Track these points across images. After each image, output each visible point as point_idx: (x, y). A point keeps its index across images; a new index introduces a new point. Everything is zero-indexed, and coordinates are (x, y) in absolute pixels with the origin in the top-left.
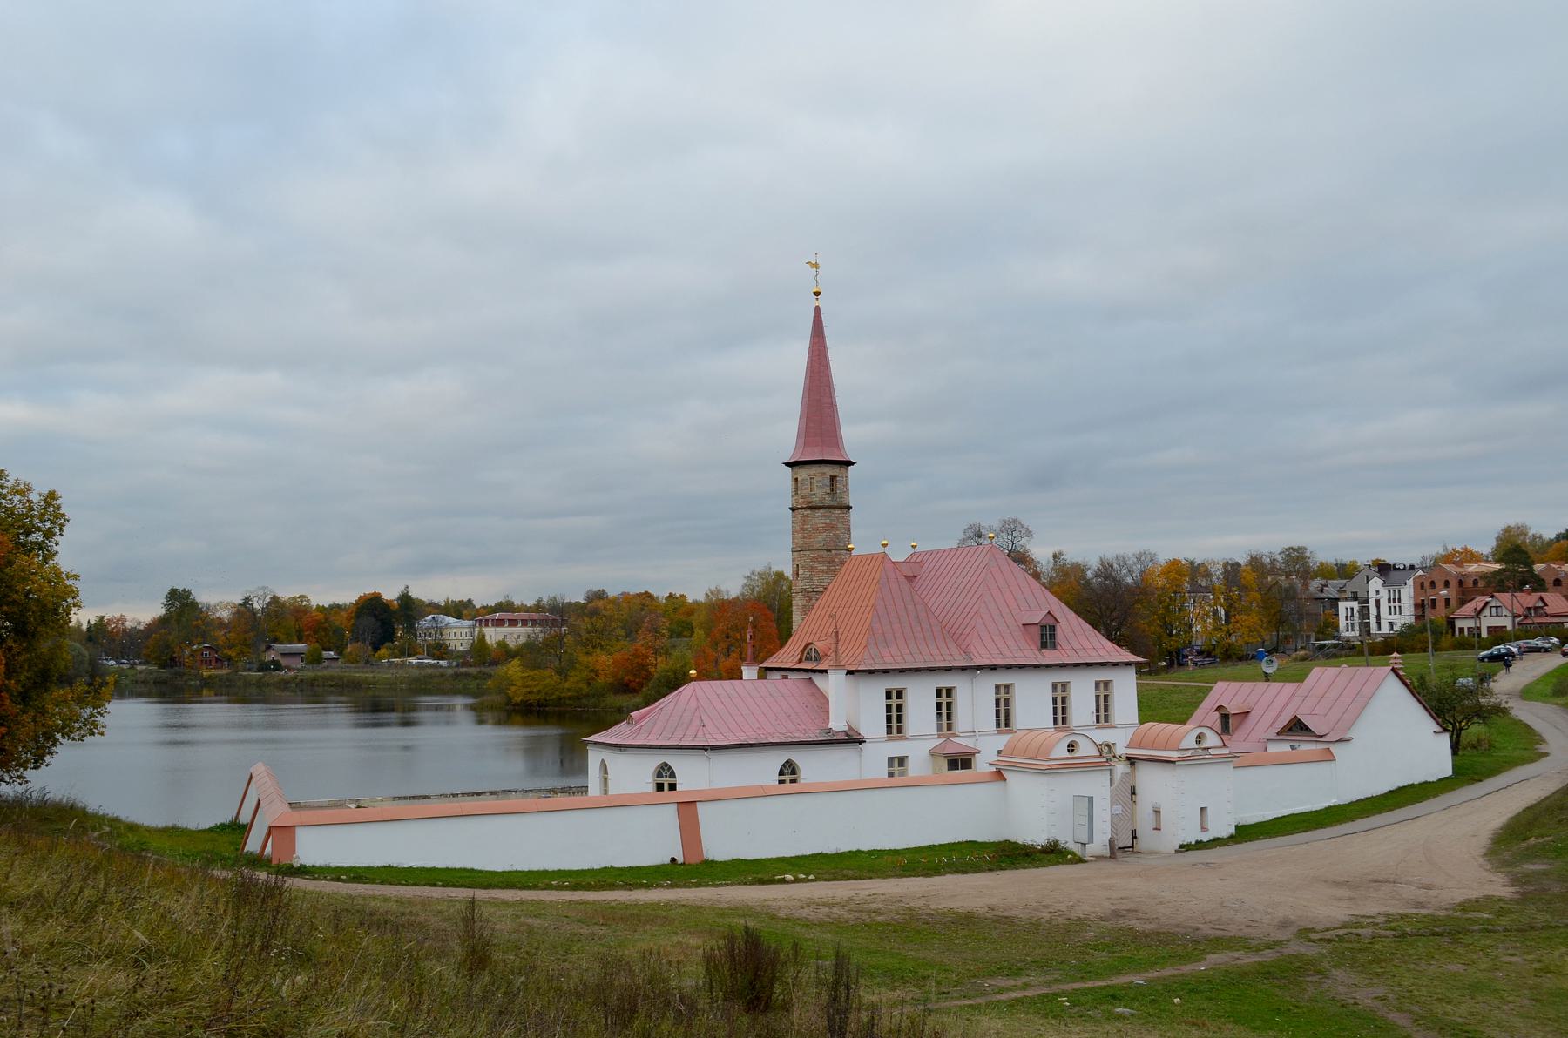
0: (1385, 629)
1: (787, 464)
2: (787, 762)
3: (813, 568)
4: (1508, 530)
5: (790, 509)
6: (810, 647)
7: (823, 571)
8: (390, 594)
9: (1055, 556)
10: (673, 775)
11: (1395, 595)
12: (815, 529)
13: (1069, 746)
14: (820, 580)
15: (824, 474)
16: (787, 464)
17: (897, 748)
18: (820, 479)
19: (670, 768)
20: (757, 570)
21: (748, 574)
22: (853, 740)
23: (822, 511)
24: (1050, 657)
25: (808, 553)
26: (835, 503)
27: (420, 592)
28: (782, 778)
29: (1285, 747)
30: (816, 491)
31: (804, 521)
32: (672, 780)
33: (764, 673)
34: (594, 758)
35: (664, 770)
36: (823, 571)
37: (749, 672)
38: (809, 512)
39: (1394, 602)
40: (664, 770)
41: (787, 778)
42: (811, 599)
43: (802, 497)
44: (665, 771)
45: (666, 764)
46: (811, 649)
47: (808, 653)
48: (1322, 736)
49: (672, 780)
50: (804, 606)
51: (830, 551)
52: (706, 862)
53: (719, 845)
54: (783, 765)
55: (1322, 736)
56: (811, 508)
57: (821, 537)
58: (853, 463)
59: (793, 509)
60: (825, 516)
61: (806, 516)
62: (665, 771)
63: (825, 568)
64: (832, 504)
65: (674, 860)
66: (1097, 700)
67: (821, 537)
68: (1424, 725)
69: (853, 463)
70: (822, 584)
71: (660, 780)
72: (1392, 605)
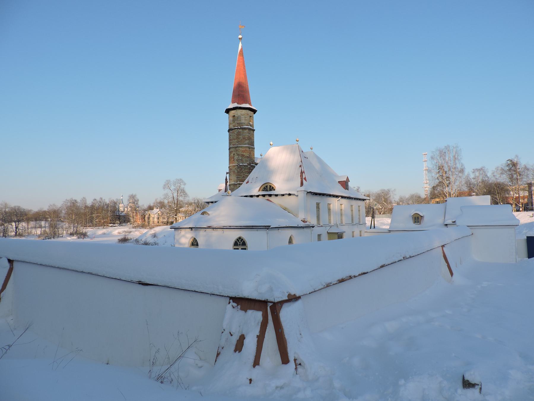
15: (248, 114)
18: (245, 116)
19: (242, 239)
20: (68, 199)
23: (247, 130)
25: (240, 148)
31: (239, 134)
35: (238, 241)
38: (241, 130)
40: (238, 241)
42: (242, 169)
43: (238, 124)
46: (267, 186)
47: (264, 188)
50: (238, 172)
60: (249, 133)
61: (240, 132)
63: (248, 155)
70: (247, 162)
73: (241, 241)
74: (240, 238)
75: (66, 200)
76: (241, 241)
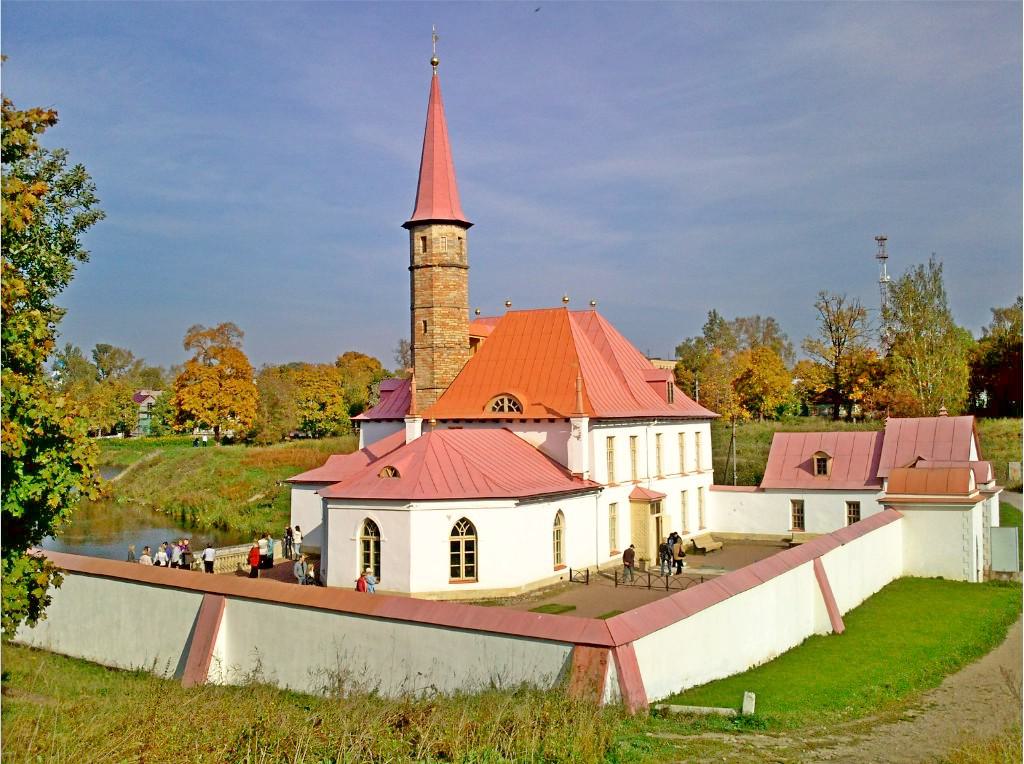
3: (444, 325)
6: (501, 397)
7: (454, 328)
10: (471, 530)
12: (446, 287)
14: (451, 336)
15: (454, 234)
32: (471, 538)
35: (459, 526)
36: (454, 328)
38: (440, 269)
40: (459, 526)
42: (442, 354)
44: (466, 526)
46: (502, 401)
47: (497, 404)
49: (471, 538)
56: (442, 266)
57: (453, 294)
67: (453, 294)
71: (456, 539)
73: (465, 526)
74: (463, 520)
76: (465, 526)
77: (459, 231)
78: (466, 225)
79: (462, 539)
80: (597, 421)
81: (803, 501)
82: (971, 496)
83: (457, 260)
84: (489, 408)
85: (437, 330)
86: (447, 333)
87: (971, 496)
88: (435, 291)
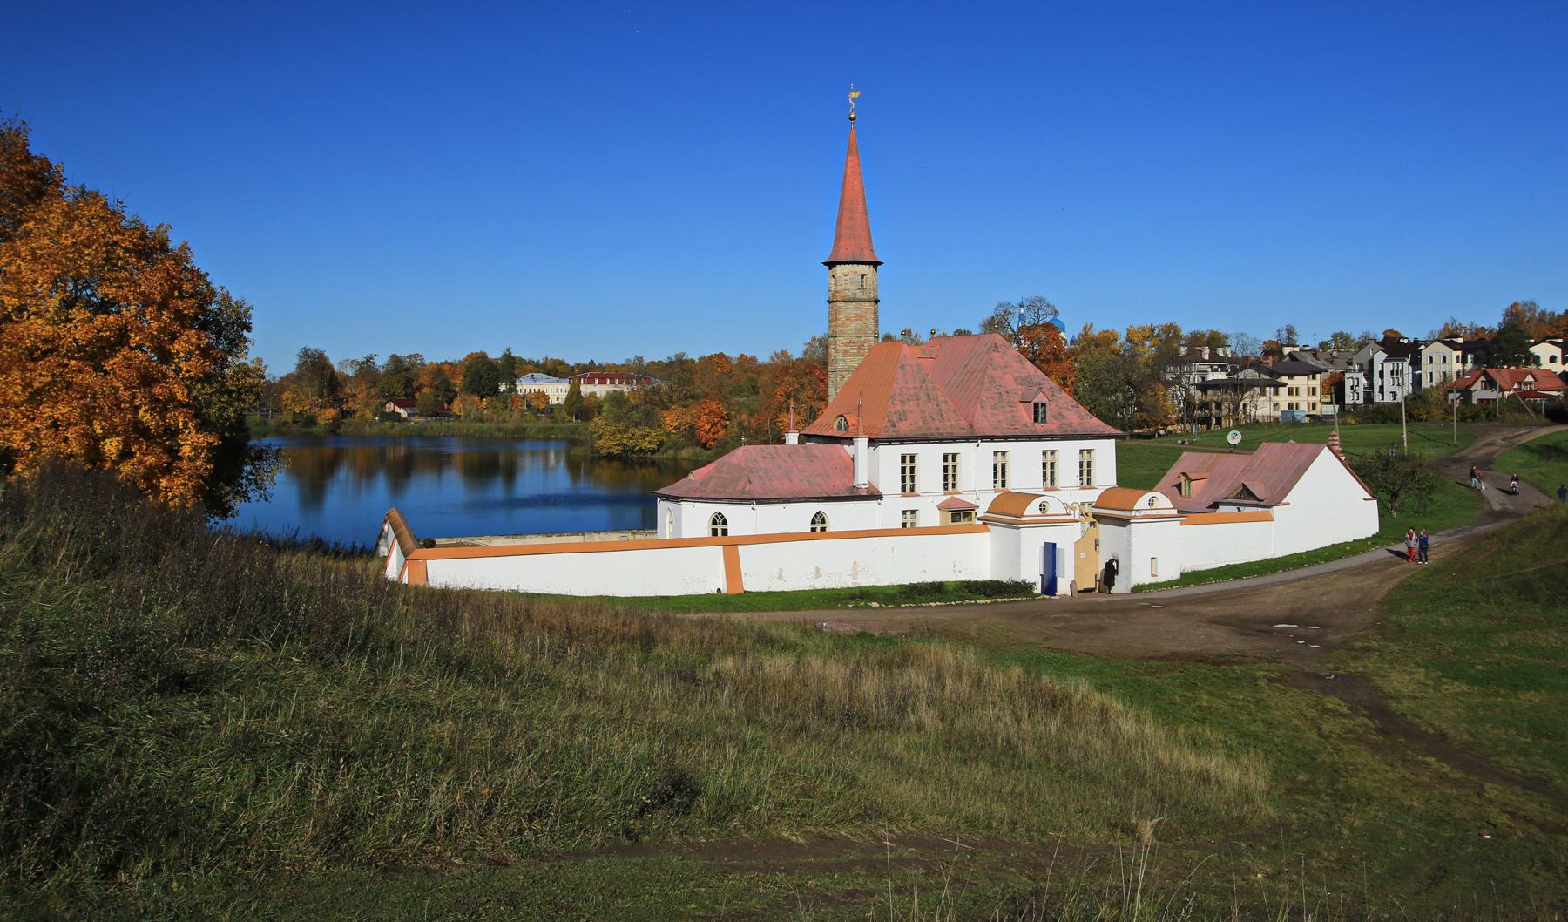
0: (1388, 398)
1: (825, 264)
2: (818, 513)
4: (1514, 306)
5: (828, 301)
6: (839, 419)
8: (495, 354)
9: (1085, 329)
10: (725, 522)
11: (1398, 367)
13: (1041, 505)
15: (855, 273)
16: (825, 264)
17: (909, 503)
19: (723, 516)
20: (817, 337)
21: (809, 340)
22: (874, 495)
23: (854, 303)
24: (1039, 428)
26: (865, 297)
27: (520, 352)
28: (814, 526)
29: (1234, 509)
30: (848, 287)
32: (724, 527)
33: (805, 438)
34: (663, 507)
37: (792, 439)
38: (843, 304)
39: (1397, 374)
41: (818, 526)
44: (718, 519)
45: (720, 514)
48: (1262, 501)
49: (724, 527)
51: (860, 337)
52: (745, 592)
53: (754, 582)
54: (815, 516)
55: (1262, 501)
57: (853, 325)
58: (881, 263)
59: (829, 302)
62: (718, 519)
64: (862, 297)
65: (719, 590)
66: (1081, 465)
68: (1354, 492)
69: (881, 263)
71: (715, 527)
72: (1394, 376)
75: (814, 339)
77: (868, 269)
78: (876, 264)
79: (720, 528)
80: (873, 442)
81: (953, 521)
82: (1023, 519)
83: (859, 295)
84: (835, 427)
85: (841, 356)
86: (848, 359)
87: (1023, 519)
88: (839, 323)
